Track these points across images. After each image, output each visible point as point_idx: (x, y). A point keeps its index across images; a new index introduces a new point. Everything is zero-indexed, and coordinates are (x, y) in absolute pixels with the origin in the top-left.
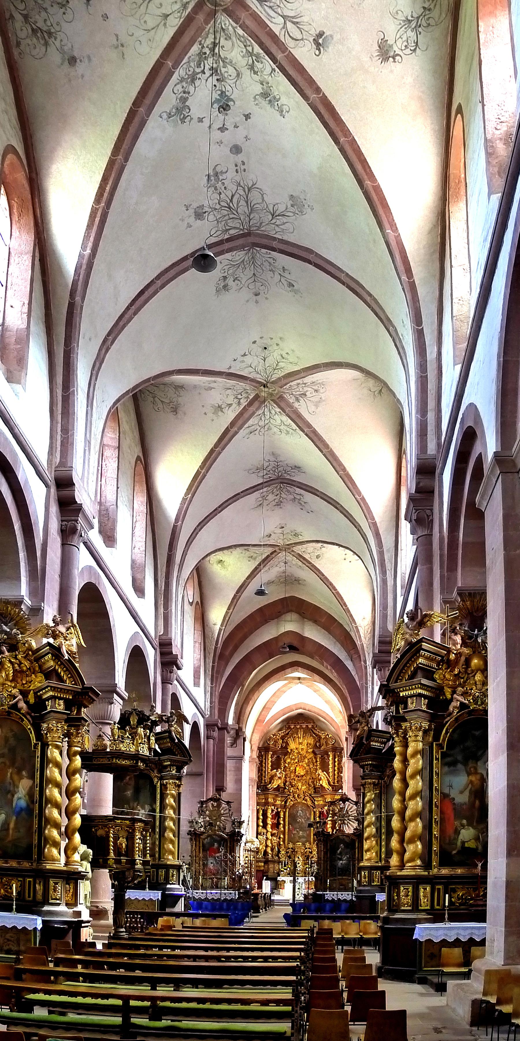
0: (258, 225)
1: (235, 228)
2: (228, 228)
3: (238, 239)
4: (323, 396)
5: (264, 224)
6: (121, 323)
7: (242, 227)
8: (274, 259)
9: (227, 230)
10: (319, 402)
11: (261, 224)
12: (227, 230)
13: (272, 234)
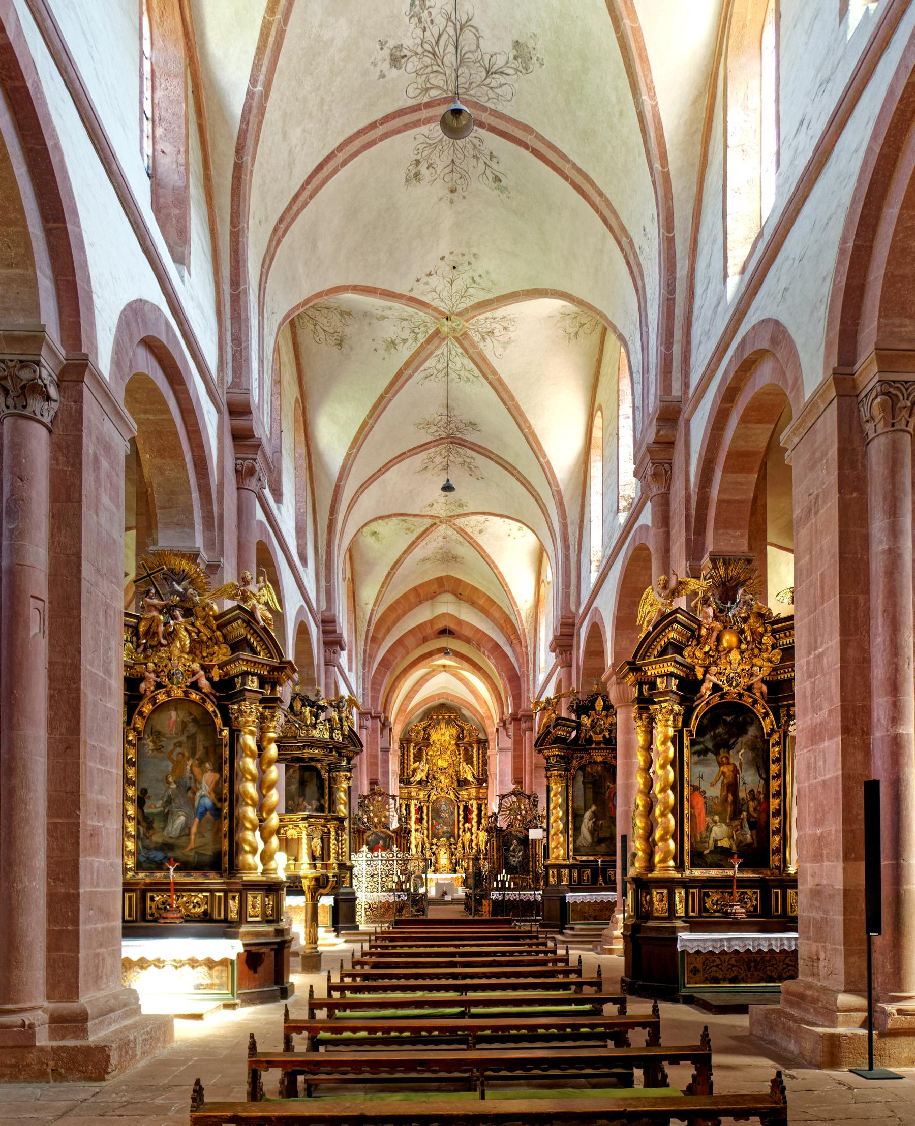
0: (467, 86)
1: (438, 87)
2: (428, 86)
3: (439, 104)
4: (512, 335)
5: (474, 85)
6: (295, 208)
7: (445, 88)
8: (480, 140)
9: (427, 89)
10: (508, 343)
11: (471, 84)
12: (427, 89)
13: (482, 100)
